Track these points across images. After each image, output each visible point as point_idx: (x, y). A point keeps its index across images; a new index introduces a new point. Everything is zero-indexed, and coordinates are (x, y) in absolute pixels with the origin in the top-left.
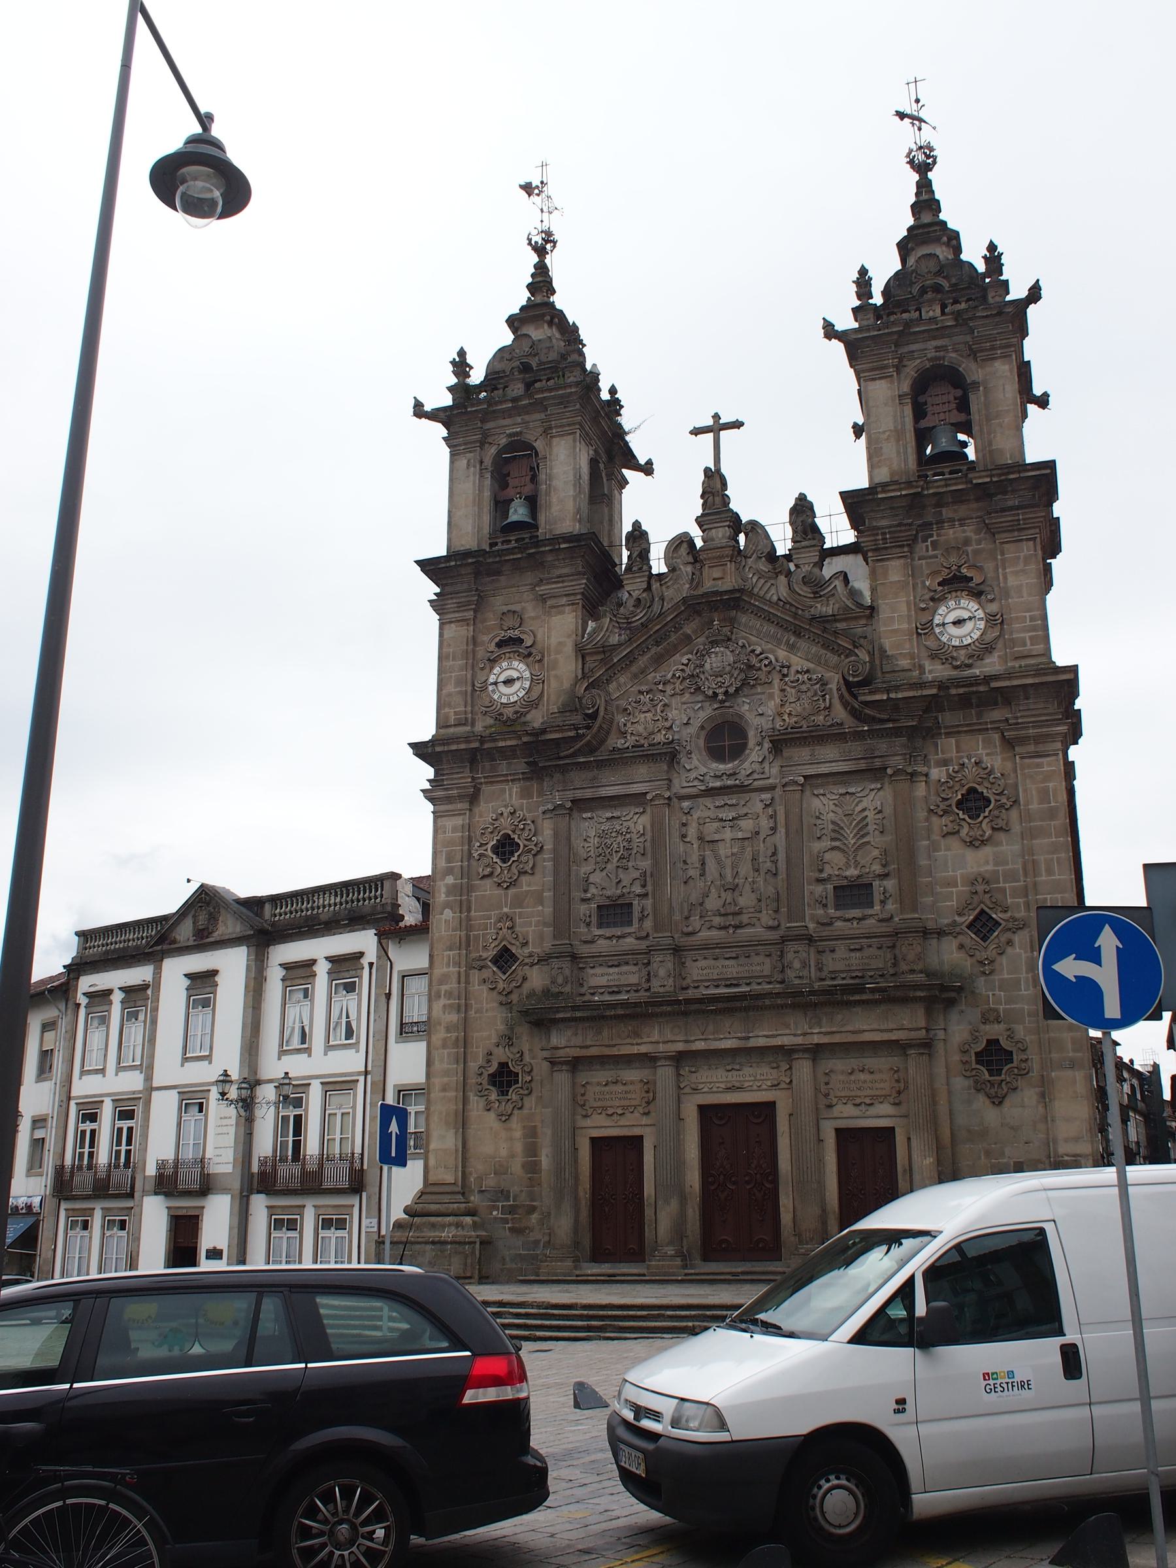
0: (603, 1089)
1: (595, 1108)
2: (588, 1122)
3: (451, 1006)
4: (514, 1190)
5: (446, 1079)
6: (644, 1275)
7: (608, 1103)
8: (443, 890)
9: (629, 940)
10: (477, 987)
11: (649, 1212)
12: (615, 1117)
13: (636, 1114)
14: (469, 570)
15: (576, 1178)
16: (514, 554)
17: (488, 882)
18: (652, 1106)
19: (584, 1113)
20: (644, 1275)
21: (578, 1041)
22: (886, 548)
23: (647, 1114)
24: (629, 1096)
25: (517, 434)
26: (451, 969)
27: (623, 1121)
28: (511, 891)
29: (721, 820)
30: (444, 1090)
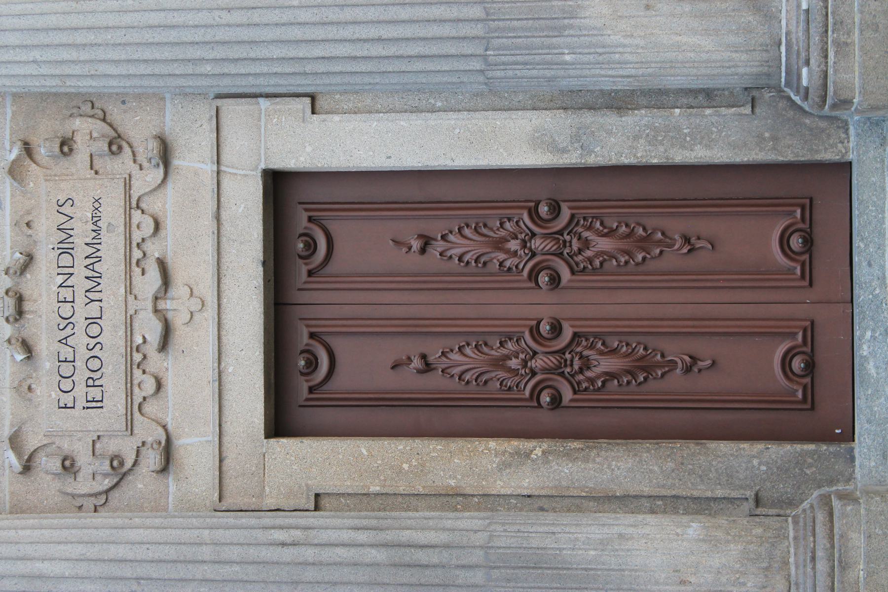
0: (46, 363)
1: (134, 408)
2: (195, 447)
7: (113, 338)
11: (619, 141)
12: (178, 305)
13: (168, 203)
15: (453, 499)
18: (139, 128)
19: (152, 459)
24: (82, 233)
27: (193, 269)
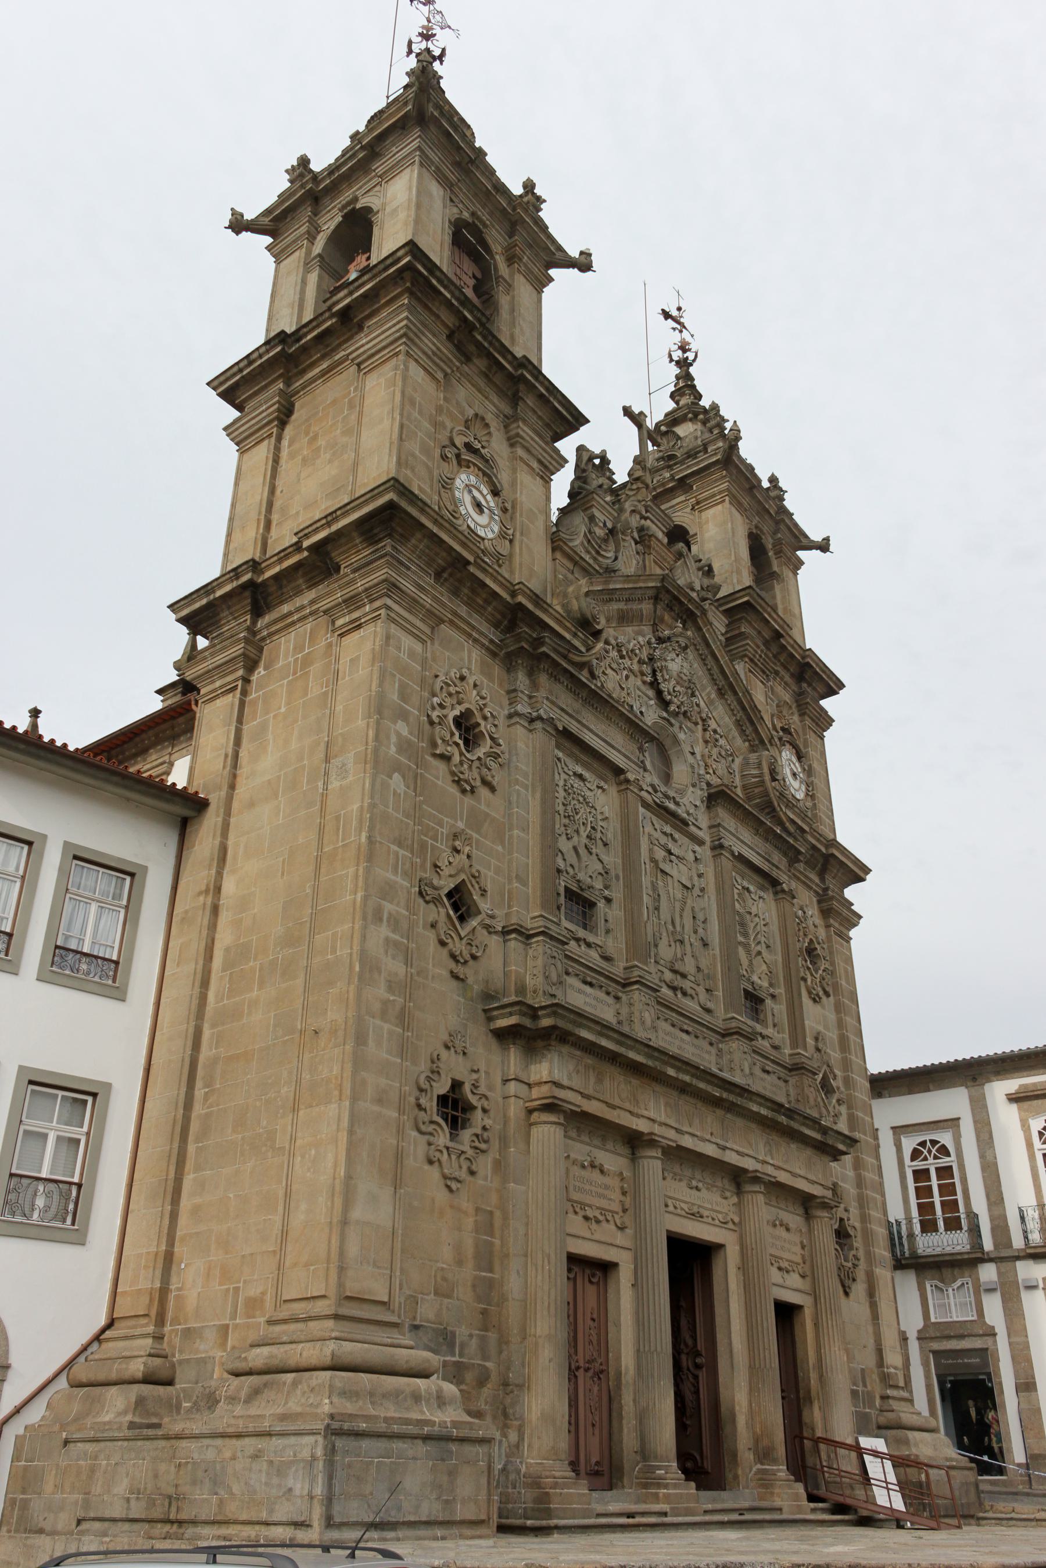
3: (396, 944)
4: (462, 1332)
5: (383, 1081)
6: (665, 1514)
7: (588, 1199)
8: (394, 739)
9: (594, 954)
10: (420, 930)
14: (450, 320)
16: (504, 357)
17: (441, 766)
20: (665, 1514)
21: (576, 1082)
22: (756, 665)
23: (621, 1229)
25: (485, 225)
26: (399, 879)
28: (468, 800)
29: (670, 853)
30: (380, 1101)
